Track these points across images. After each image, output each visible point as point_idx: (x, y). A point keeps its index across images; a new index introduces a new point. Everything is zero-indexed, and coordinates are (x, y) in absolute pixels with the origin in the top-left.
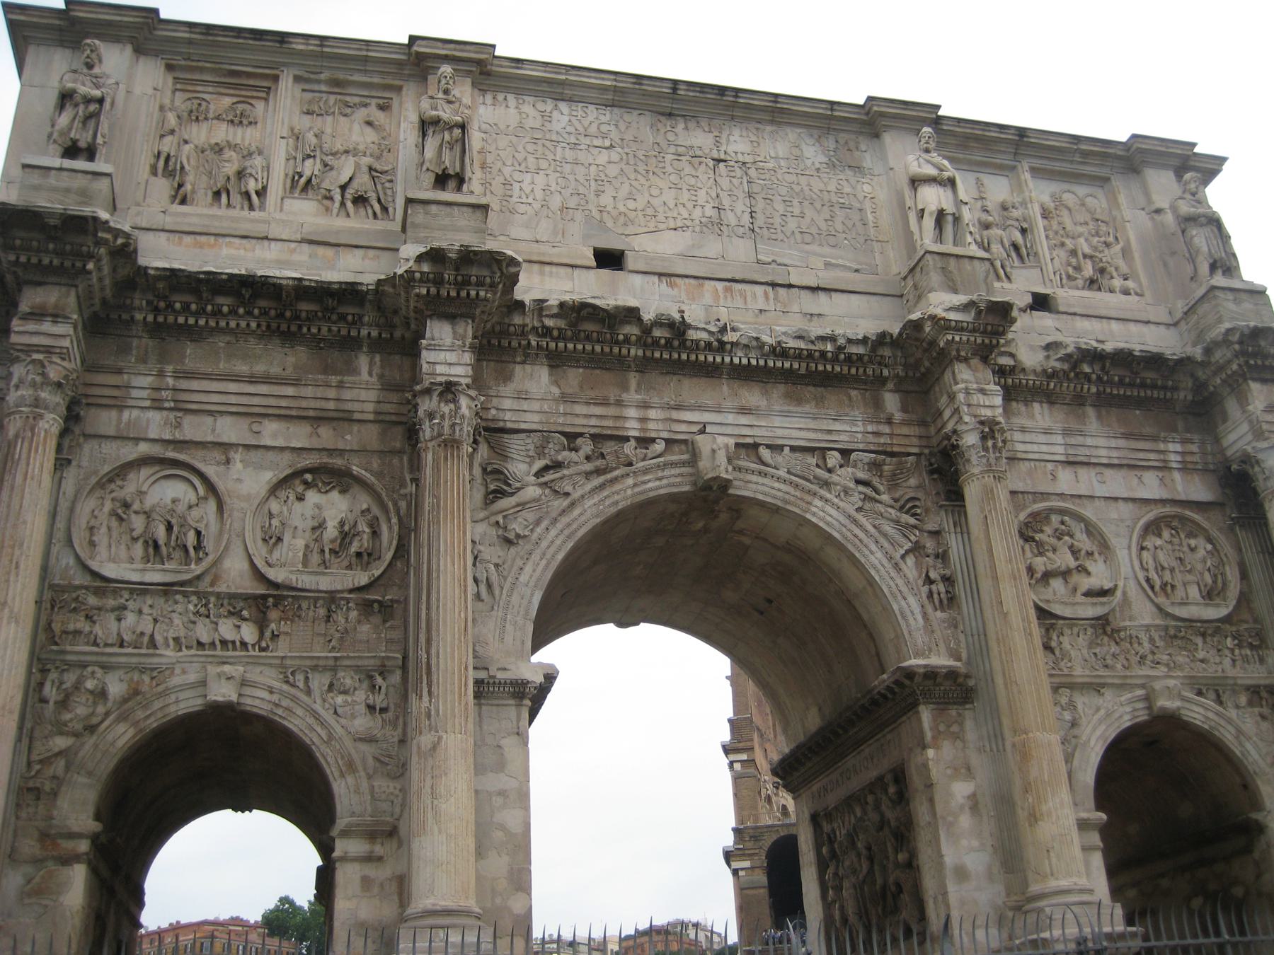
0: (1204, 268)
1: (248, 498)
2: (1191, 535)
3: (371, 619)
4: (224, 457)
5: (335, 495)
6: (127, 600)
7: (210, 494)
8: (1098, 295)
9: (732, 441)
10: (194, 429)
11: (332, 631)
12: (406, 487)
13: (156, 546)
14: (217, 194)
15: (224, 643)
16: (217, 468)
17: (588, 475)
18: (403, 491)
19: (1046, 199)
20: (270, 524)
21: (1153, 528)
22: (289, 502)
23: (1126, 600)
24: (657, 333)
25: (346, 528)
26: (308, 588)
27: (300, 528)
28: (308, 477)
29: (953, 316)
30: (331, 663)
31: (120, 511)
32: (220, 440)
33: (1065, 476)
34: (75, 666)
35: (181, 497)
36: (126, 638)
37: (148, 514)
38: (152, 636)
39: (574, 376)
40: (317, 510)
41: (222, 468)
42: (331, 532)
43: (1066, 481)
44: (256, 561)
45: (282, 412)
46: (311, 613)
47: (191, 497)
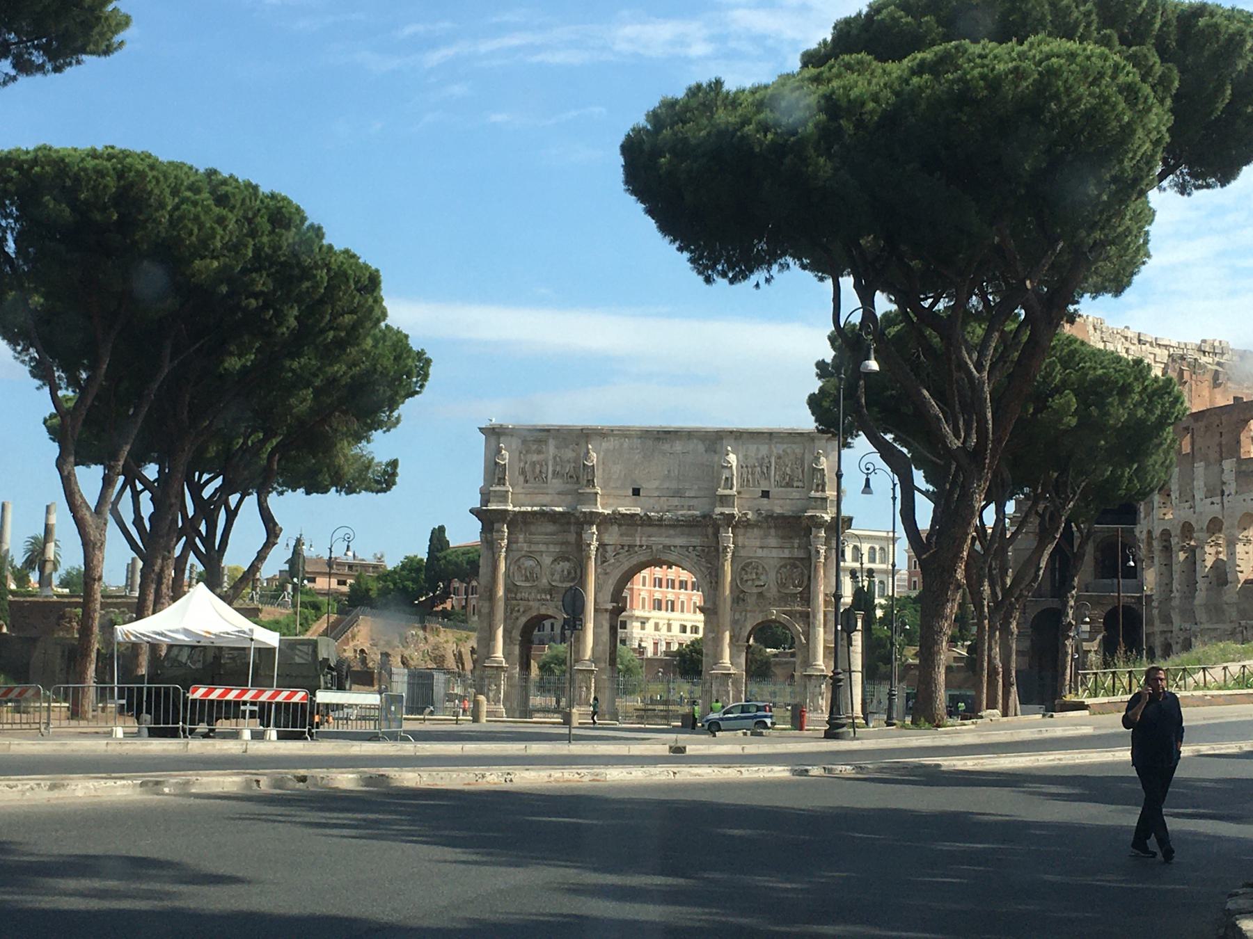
0: (814, 487)
2: (796, 568)
5: (566, 563)
8: (789, 489)
9: (661, 546)
10: (534, 548)
14: (535, 479)
15: (544, 600)
17: (626, 556)
19: (781, 452)
21: (785, 566)
23: (769, 588)
24: (644, 518)
29: (718, 517)
33: (760, 551)
37: (526, 569)
39: (624, 527)
42: (566, 572)
43: (760, 553)
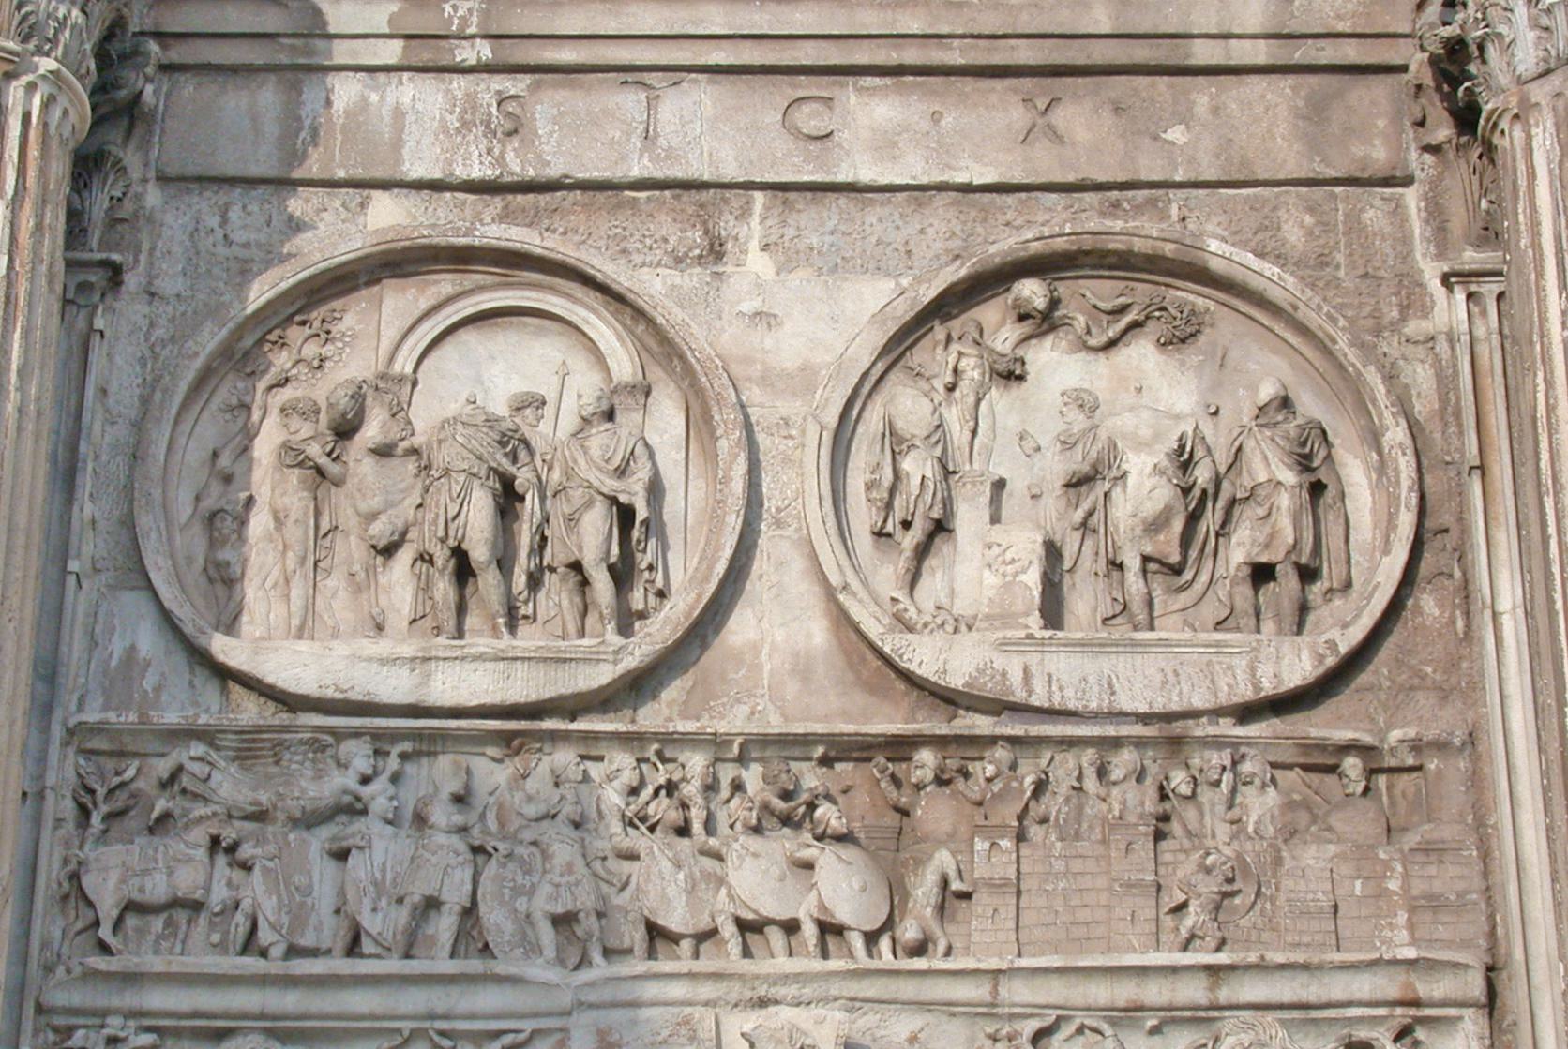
1: (803, 381)
3: (1336, 820)
4: (698, 234)
5: (1141, 354)
6: (365, 780)
7: (656, 373)
11: (1187, 868)
12: (1426, 312)
13: (463, 569)
16: (675, 277)
18: (1414, 327)
20: (897, 475)
22: (965, 387)
25: (1202, 475)
26: (1071, 705)
27: (1017, 486)
28: (1031, 291)
30: (1193, 991)
31: (315, 450)
32: (677, 172)
34: (177, 1033)
35: (548, 391)
36: (370, 923)
38: (470, 912)
40: (1078, 421)
41: (693, 278)
44: (856, 612)
45: (911, 55)
46: (1093, 809)
47: (584, 387)
